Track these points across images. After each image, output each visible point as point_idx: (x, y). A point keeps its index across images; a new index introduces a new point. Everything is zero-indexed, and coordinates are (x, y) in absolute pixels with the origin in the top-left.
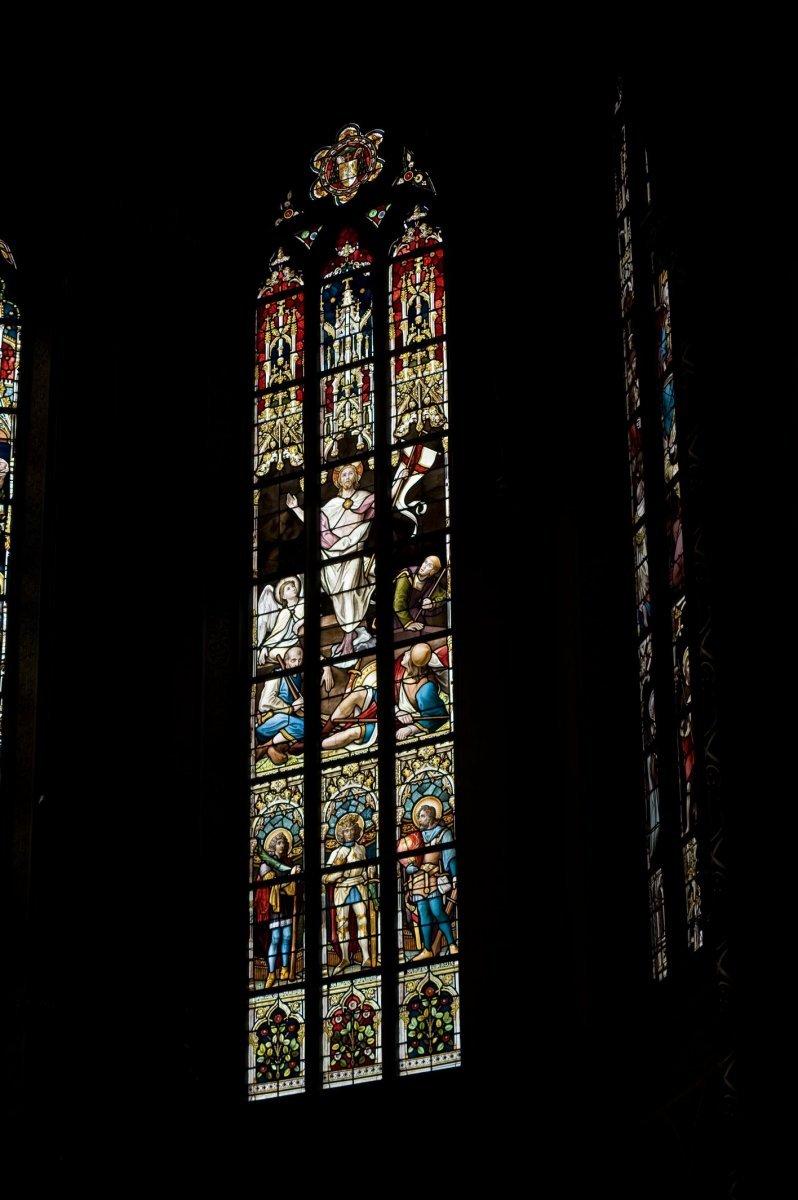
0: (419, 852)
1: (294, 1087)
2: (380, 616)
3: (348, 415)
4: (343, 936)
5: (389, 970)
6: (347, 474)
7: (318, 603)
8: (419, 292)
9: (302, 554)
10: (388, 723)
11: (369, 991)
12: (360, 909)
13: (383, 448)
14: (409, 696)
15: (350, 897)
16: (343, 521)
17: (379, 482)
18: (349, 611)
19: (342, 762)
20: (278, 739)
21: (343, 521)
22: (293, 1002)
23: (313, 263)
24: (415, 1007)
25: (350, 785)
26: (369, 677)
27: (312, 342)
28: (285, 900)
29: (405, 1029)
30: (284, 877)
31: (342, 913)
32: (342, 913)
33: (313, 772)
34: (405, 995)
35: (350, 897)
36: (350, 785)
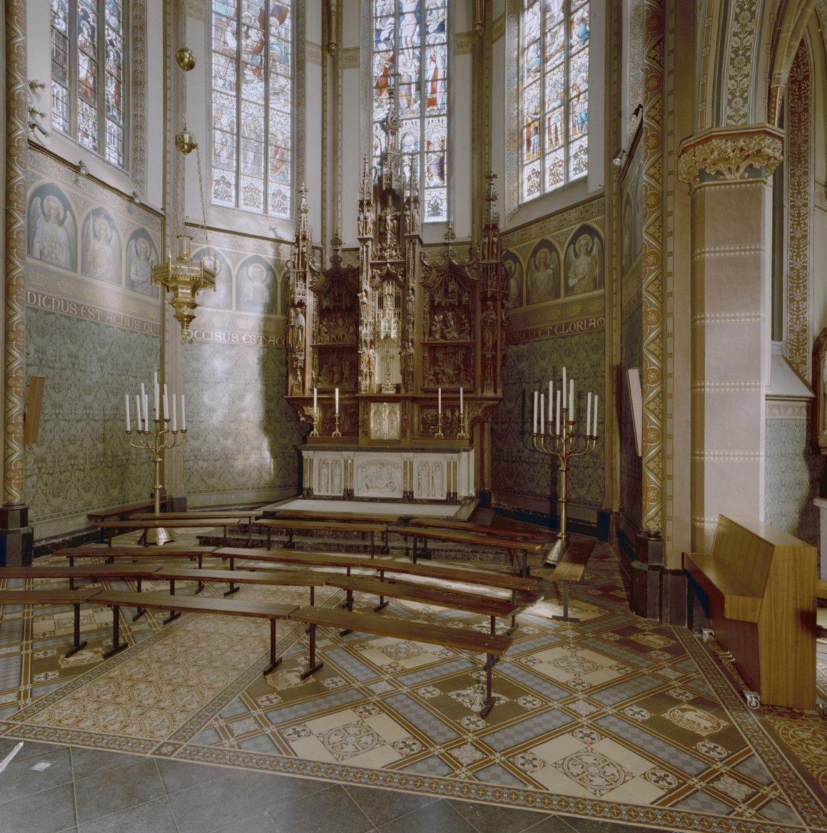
0: (578, 96)
4: (553, 136)
10: (567, 47)
11: (561, 154)
12: (558, 124)
19: (554, 69)
20: (534, 68)
24: (576, 156)
26: (562, 31)
28: (536, 128)
30: (536, 120)
31: (553, 128)
32: (553, 128)
34: (572, 153)
36: (555, 78)
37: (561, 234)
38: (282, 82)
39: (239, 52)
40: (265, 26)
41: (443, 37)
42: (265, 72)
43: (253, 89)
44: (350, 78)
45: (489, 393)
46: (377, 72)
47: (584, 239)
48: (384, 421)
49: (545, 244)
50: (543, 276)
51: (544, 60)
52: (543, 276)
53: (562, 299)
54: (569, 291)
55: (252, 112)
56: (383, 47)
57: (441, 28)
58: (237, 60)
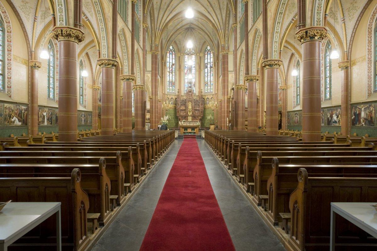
1: (207, 91)
2: (210, 71)
3: (209, 61)
5: (210, 87)
6: (209, 64)
7: (208, 70)
8: (212, 54)
9: (207, 67)
13: (210, 63)
14: (211, 74)
15: (209, 83)
16: (209, 66)
18: (209, 70)
21: (209, 66)
22: (207, 88)
23: (208, 52)
25: (209, 78)
27: (207, 57)
29: (211, 89)
33: (208, 78)
36: (209, 78)
37: (210, 97)
38: (174, 74)
41: (194, 68)
42: (172, 73)
43: (171, 75)
44: (182, 73)
45: (202, 115)
46: (185, 72)
48: (190, 119)
49: (208, 98)
51: (208, 76)
55: (171, 78)
56: (186, 69)
57: (194, 67)
58: (169, 72)
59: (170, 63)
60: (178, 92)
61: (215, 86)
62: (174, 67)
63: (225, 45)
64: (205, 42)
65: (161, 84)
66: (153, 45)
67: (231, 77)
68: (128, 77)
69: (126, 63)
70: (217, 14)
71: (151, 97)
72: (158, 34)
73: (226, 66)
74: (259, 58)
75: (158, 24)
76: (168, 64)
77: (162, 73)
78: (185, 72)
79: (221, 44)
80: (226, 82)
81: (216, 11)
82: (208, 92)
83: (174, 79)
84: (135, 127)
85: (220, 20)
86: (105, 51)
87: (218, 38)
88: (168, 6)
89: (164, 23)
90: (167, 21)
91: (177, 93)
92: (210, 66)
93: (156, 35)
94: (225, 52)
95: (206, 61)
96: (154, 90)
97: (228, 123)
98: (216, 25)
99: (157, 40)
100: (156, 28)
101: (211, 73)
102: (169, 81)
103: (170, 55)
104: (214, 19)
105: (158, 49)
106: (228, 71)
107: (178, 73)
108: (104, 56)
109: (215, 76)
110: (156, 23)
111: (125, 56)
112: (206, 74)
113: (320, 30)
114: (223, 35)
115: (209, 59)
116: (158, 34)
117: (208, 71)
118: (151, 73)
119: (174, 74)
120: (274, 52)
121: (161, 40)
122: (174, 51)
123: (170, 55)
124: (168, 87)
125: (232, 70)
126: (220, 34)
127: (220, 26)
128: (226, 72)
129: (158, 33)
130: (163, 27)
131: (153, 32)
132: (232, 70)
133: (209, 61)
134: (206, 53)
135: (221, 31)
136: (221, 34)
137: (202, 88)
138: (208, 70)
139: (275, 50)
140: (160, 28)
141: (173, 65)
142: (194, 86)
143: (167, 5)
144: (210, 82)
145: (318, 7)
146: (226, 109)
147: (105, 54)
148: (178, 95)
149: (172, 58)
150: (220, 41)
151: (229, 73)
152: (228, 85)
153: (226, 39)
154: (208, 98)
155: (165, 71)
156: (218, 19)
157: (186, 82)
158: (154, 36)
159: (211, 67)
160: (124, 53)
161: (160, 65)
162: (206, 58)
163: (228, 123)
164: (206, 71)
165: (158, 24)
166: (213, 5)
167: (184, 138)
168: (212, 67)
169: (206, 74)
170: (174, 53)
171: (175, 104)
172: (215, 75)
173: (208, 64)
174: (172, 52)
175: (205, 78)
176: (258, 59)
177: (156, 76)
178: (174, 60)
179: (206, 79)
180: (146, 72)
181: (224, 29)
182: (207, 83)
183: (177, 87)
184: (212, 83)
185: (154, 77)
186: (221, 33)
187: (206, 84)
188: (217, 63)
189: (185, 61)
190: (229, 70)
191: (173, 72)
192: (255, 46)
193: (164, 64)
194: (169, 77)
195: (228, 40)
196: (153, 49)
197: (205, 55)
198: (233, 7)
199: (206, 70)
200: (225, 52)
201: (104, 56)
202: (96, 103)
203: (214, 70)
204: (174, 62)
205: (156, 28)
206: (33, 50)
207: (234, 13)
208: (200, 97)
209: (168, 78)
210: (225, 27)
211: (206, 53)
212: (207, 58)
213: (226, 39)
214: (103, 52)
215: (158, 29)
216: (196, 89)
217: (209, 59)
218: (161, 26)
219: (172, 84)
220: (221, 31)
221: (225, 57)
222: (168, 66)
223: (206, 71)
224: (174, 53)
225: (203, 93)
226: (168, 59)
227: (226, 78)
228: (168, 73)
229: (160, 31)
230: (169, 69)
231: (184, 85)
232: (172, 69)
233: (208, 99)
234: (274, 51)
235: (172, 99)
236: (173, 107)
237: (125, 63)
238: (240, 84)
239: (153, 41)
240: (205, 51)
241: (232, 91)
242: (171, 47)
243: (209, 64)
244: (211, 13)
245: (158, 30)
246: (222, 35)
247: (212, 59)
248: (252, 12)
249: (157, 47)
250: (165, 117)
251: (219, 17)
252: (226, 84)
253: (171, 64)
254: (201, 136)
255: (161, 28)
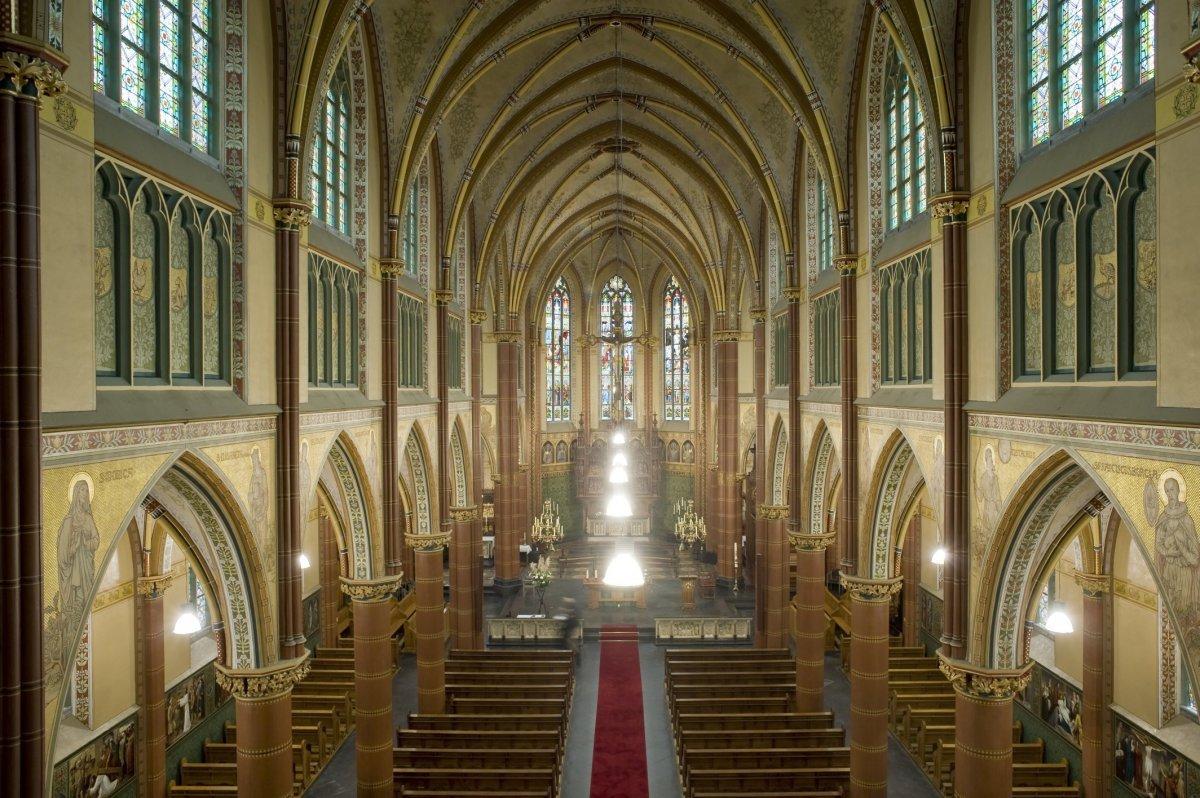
1: (670, 418)
2: (682, 355)
3: (677, 322)
7: (674, 350)
8: (685, 304)
9: (670, 342)
11: (680, 407)
14: (685, 366)
15: (678, 393)
16: (677, 339)
17: (681, 333)
18: (678, 352)
21: (677, 339)
23: (673, 295)
25: (677, 378)
26: (679, 363)
27: (672, 309)
33: (673, 375)
35: (678, 393)
36: (677, 378)
38: (566, 363)
39: (553, 356)
40: (561, 341)
42: (561, 361)
43: (557, 370)
46: (603, 354)
47: (688, 445)
49: (674, 441)
50: (674, 453)
52: (674, 453)
53: (681, 463)
54: (683, 461)
58: (553, 361)
59: (553, 329)
60: (581, 423)
61: (697, 404)
62: (566, 341)
63: (727, 315)
64: (661, 265)
65: (527, 417)
66: (502, 317)
67: (746, 411)
68: (430, 543)
69: (422, 502)
70: (703, 220)
71: (499, 479)
72: (519, 280)
73: (730, 361)
74: (832, 480)
75: (518, 253)
76: (549, 333)
77: (531, 382)
78: (603, 354)
79: (715, 308)
80: (731, 427)
81: (698, 212)
82: (673, 420)
83: (566, 379)
84: (452, 564)
85: (712, 242)
86: (364, 560)
87: (707, 290)
88: (548, 200)
89: (536, 245)
90: (544, 239)
91: (578, 426)
92: (682, 340)
93: (509, 286)
94: (727, 337)
95: (668, 320)
96: (506, 455)
97: (736, 558)
98: (698, 249)
99: (515, 298)
100: (509, 264)
101: (685, 361)
102: (553, 390)
103: (553, 305)
104: (691, 234)
105: (517, 324)
106: (736, 395)
107: (579, 359)
108: (362, 574)
109: (697, 373)
110: (510, 251)
111: (420, 482)
112: (668, 364)
113: (1008, 678)
114: (722, 282)
115: (677, 317)
116: (519, 280)
117: (673, 355)
118: (495, 401)
119: (566, 363)
120: (877, 561)
121: (526, 297)
122: (568, 291)
123: (553, 305)
124: (550, 408)
125: (751, 391)
126: (712, 278)
127: (713, 257)
128: (731, 398)
129: (515, 282)
130: (536, 251)
131: (502, 277)
132: (751, 391)
133: (677, 322)
134: (668, 297)
135: (713, 270)
136: (717, 283)
137: (656, 408)
138: (674, 350)
139: (883, 529)
140: (524, 261)
141: (564, 335)
142: (631, 400)
143: (543, 197)
144: (681, 389)
145: (1002, 657)
146: (731, 516)
147: (365, 569)
148: (581, 432)
149: (562, 315)
150: (712, 294)
151: (740, 400)
152: (736, 440)
153: (733, 296)
154: (674, 441)
155: (538, 358)
156: (705, 236)
157: (605, 387)
158: (504, 287)
159: (683, 344)
160: (417, 474)
161: (524, 358)
162: (668, 312)
163: (736, 558)
164: (669, 354)
165: (518, 253)
166: (690, 196)
167: (602, 638)
168: (688, 345)
169: (668, 364)
170: (566, 297)
171: (572, 460)
172: (697, 370)
173: (673, 334)
174: (561, 295)
175: (665, 375)
176: (831, 484)
177: (511, 393)
178: (566, 321)
179: (668, 378)
180: (482, 400)
181: (724, 263)
182: (672, 393)
183: (577, 409)
184: (686, 394)
185: (505, 416)
186: (715, 278)
187: (668, 394)
188: (704, 348)
189: (603, 320)
190: (741, 390)
191: (565, 357)
192: (817, 470)
193: (534, 334)
194: (553, 375)
195: (738, 299)
196: (503, 328)
197: (665, 301)
198: (753, 259)
199: (668, 349)
200: (727, 337)
201: (362, 574)
202: (329, 538)
203: (693, 355)
204: (566, 327)
205: (509, 264)
206: (148, 546)
207: (756, 278)
208: (649, 434)
209: (549, 378)
210: (728, 259)
211: (668, 297)
212: (672, 315)
213: (733, 296)
214: (357, 564)
215: (515, 268)
216: (636, 408)
217: (677, 317)
218: (528, 248)
219: (561, 394)
220: (713, 270)
221: (728, 353)
222: (549, 341)
223: (669, 354)
224: (566, 297)
225: (658, 426)
226: (549, 319)
227: (731, 417)
228: (549, 365)
229: (524, 270)
230: (553, 350)
231: (601, 398)
232: (561, 349)
233: (673, 444)
234: (878, 556)
235: (562, 445)
236: (565, 468)
237: (419, 502)
238: (775, 503)
239: (502, 305)
240: (666, 290)
241: (751, 455)
242: (558, 283)
243: (677, 331)
244: (685, 216)
245: (519, 270)
246: (717, 283)
247: (686, 319)
248: (811, 343)
249: (513, 319)
250: (541, 560)
251: (710, 230)
252: (731, 436)
253: (557, 334)
254: (653, 630)
255: (528, 262)
